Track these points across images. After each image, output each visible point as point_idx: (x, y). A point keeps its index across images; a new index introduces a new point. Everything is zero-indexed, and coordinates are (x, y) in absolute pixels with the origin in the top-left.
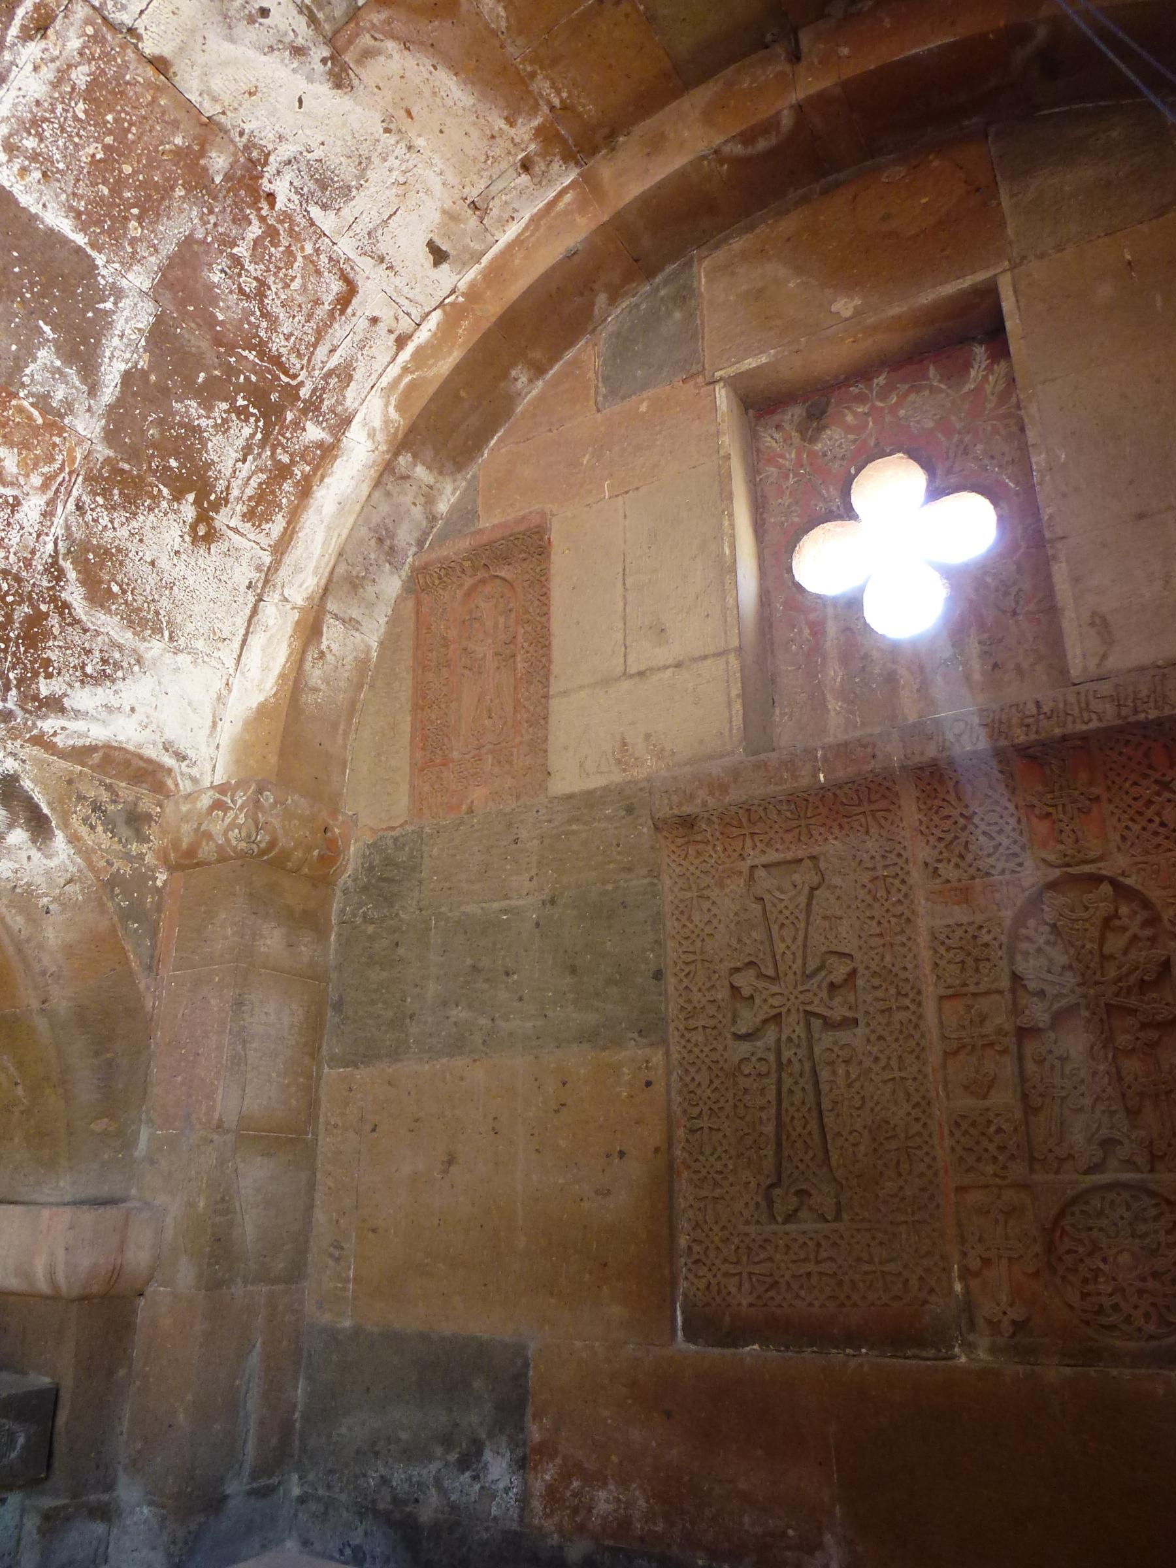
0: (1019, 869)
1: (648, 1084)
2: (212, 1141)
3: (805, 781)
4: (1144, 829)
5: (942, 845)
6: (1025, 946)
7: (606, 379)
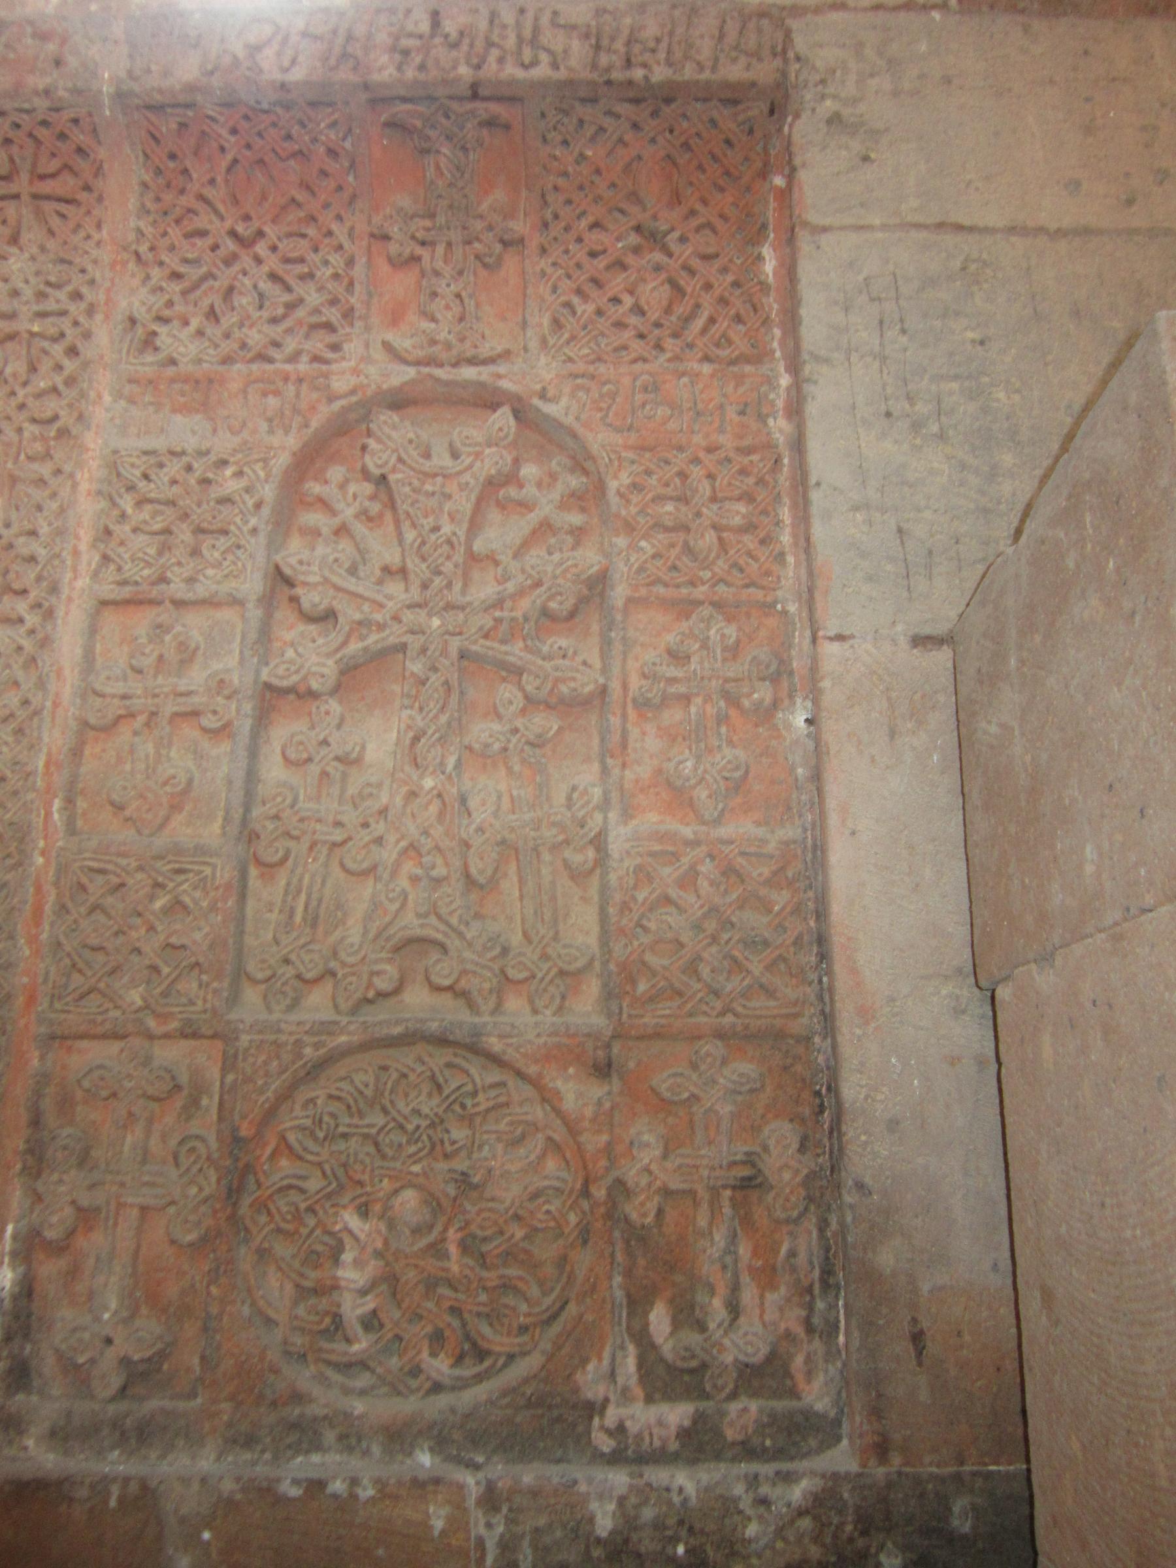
0: (330, 355)
4: (599, 312)
5: (176, 287)
6: (313, 518)
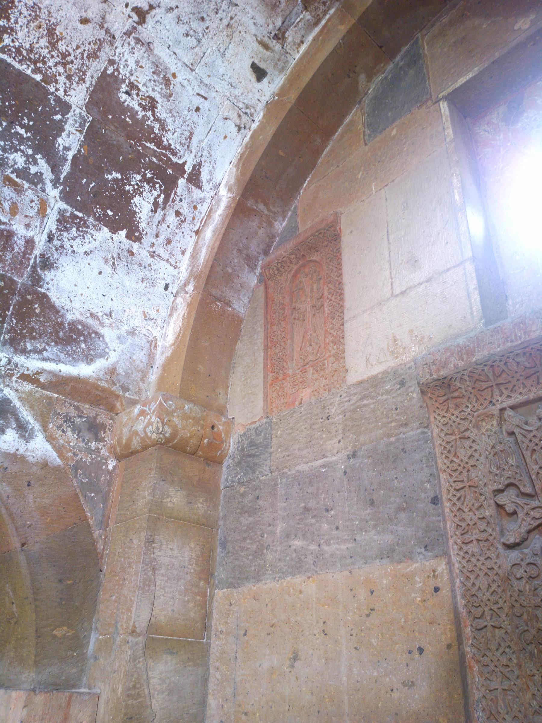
1: (437, 589)
2: (128, 642)
7: (369, 125)
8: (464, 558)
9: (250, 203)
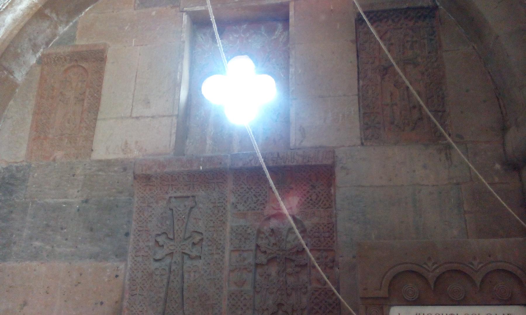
1: (117, 276)
3: (195, 168)
4: (305, 200)
5: (239, 197)
6: (262, 235)
8: (134, 263)
9: (47, 11)
